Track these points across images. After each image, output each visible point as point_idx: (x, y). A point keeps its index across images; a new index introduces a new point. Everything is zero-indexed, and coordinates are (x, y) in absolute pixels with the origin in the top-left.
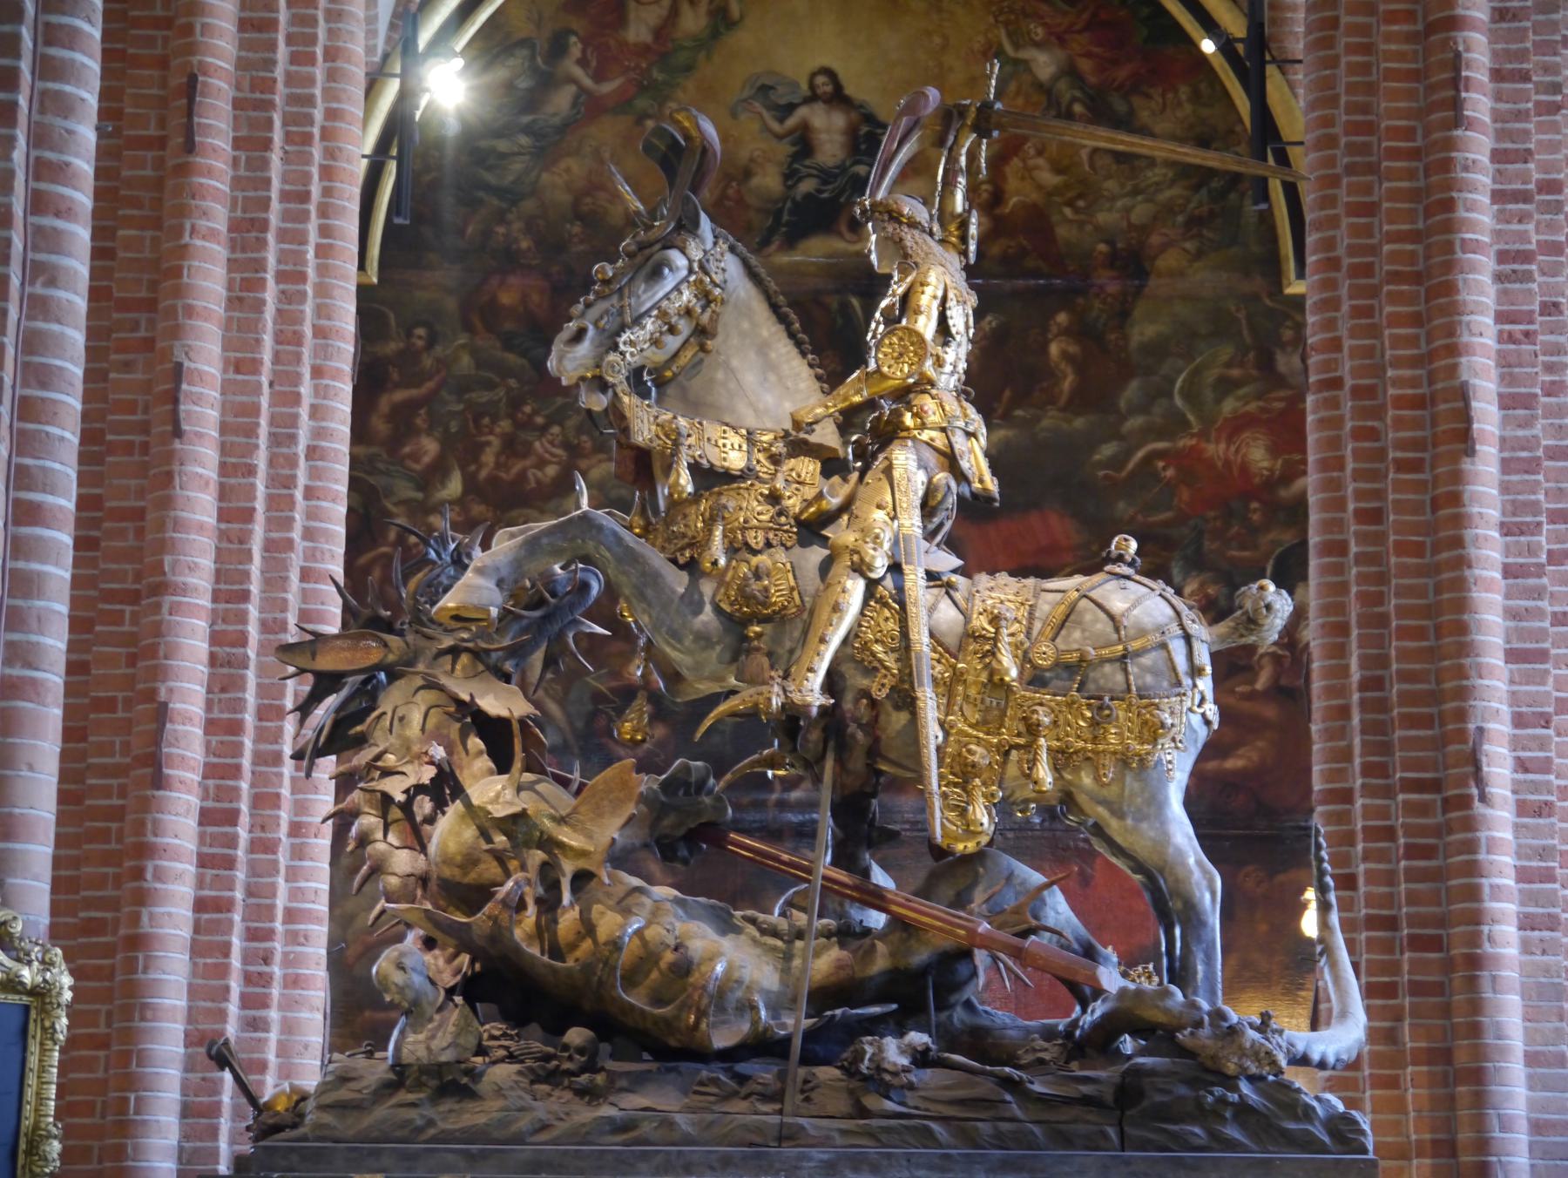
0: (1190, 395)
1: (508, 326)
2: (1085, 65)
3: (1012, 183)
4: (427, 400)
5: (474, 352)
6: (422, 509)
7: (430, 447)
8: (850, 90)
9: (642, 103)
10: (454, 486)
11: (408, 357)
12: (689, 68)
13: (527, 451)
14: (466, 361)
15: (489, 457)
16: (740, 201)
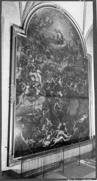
0: (80, 64)
1: (37, 46)
2: (74, 36)
3: (70, 44)
4: (31, 51)
5: (35, 47)
6: (31, 62)
7: (31, 56)
8: (61, 32)
9: (47, 27)
10: (33, 61)
11: (29, 46)
12: (51, 26)
13: (39, 59)
14: (34, 48)
15: (36, 58)
16: (54, 39)
